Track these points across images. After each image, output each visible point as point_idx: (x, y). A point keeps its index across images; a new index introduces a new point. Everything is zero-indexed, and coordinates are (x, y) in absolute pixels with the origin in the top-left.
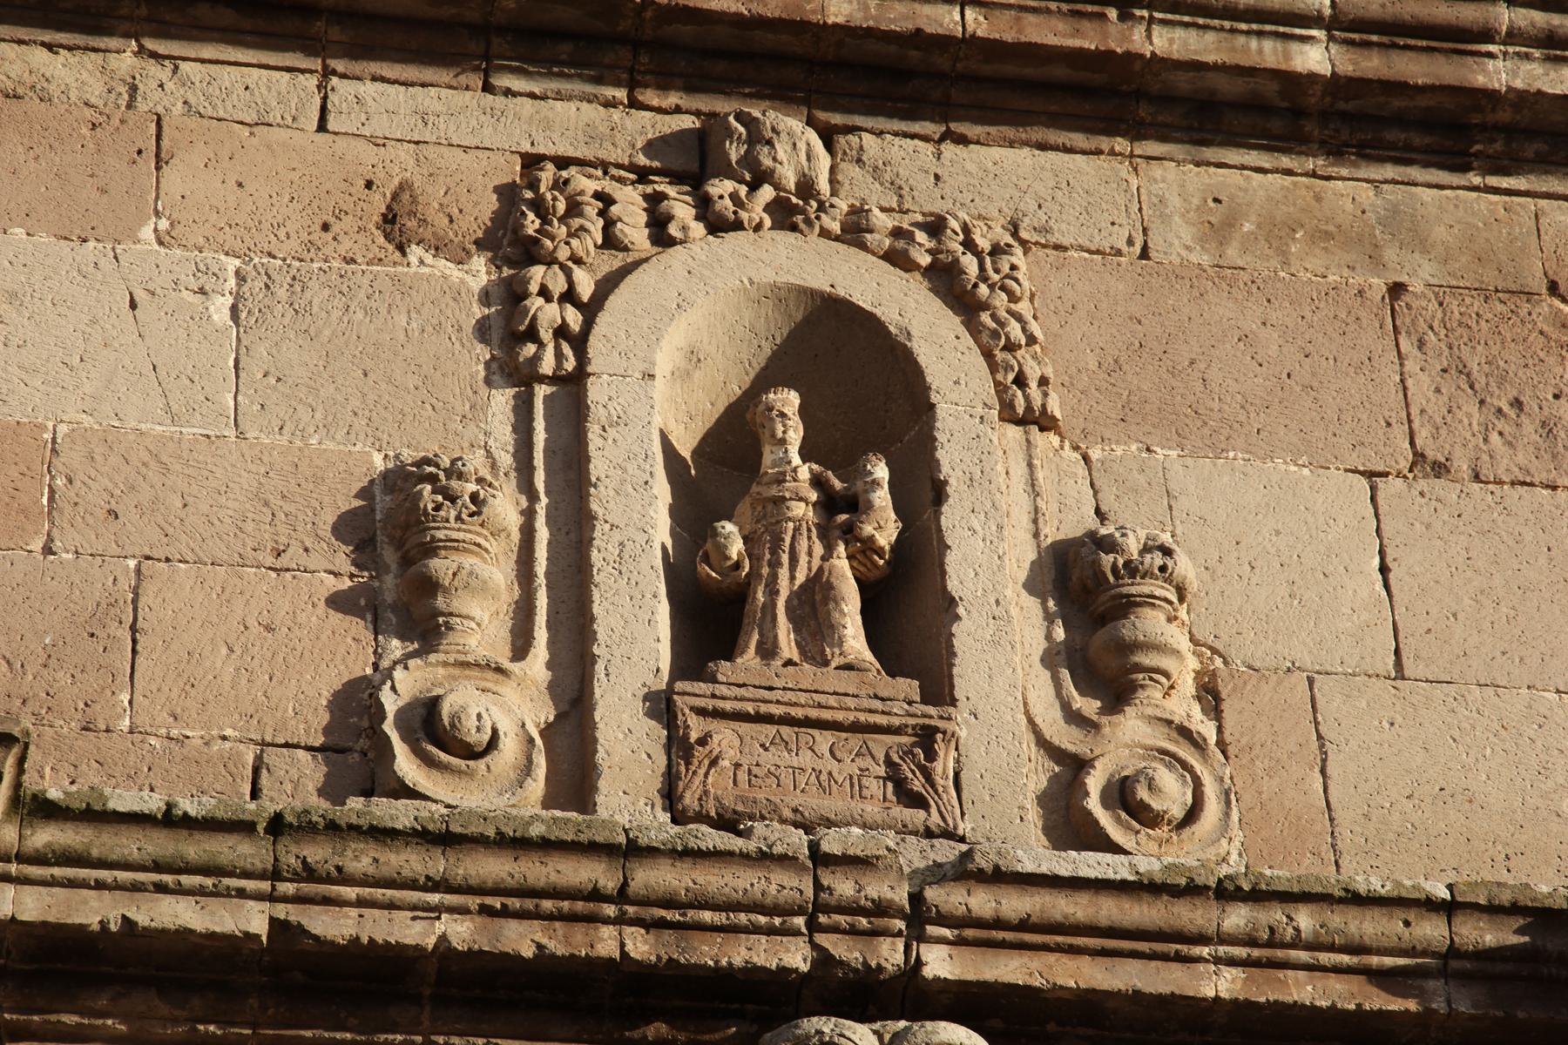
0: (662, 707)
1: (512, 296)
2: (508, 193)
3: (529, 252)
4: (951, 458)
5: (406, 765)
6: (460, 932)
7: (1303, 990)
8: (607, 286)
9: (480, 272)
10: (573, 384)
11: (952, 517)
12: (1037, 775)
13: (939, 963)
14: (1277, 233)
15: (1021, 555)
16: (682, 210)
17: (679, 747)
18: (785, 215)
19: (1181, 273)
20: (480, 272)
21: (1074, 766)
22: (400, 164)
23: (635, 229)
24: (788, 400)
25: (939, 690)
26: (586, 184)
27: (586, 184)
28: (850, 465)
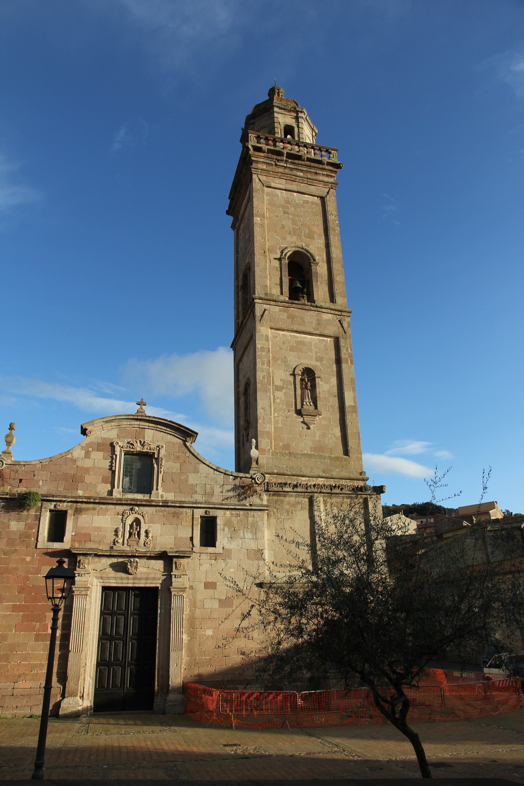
0: (127, 540)
1: (123, 518)
2: (123, 512)
3: (124, 516)
4: (142, 526)
5: (116, 544)
6: (117, 554)
7: (152, 555)
8: (127, 517)
9: (121, 517)
10: (125, 523)
11: (141, 529)
12: (143, 542)
13: (137, 555)
14: (159, 512)
15: (144, 531)
16: (131, 513)
17: (128, 542)
18: (136, 513)
19: (154, 514)
20: (121, 517)
21: (145, 542)
22: (118, 511)
23: (129, 514)
24: (135, 523)
25: (139, 539)
26: (126, 511)
27: (126, 511)
28: (137, 527)
